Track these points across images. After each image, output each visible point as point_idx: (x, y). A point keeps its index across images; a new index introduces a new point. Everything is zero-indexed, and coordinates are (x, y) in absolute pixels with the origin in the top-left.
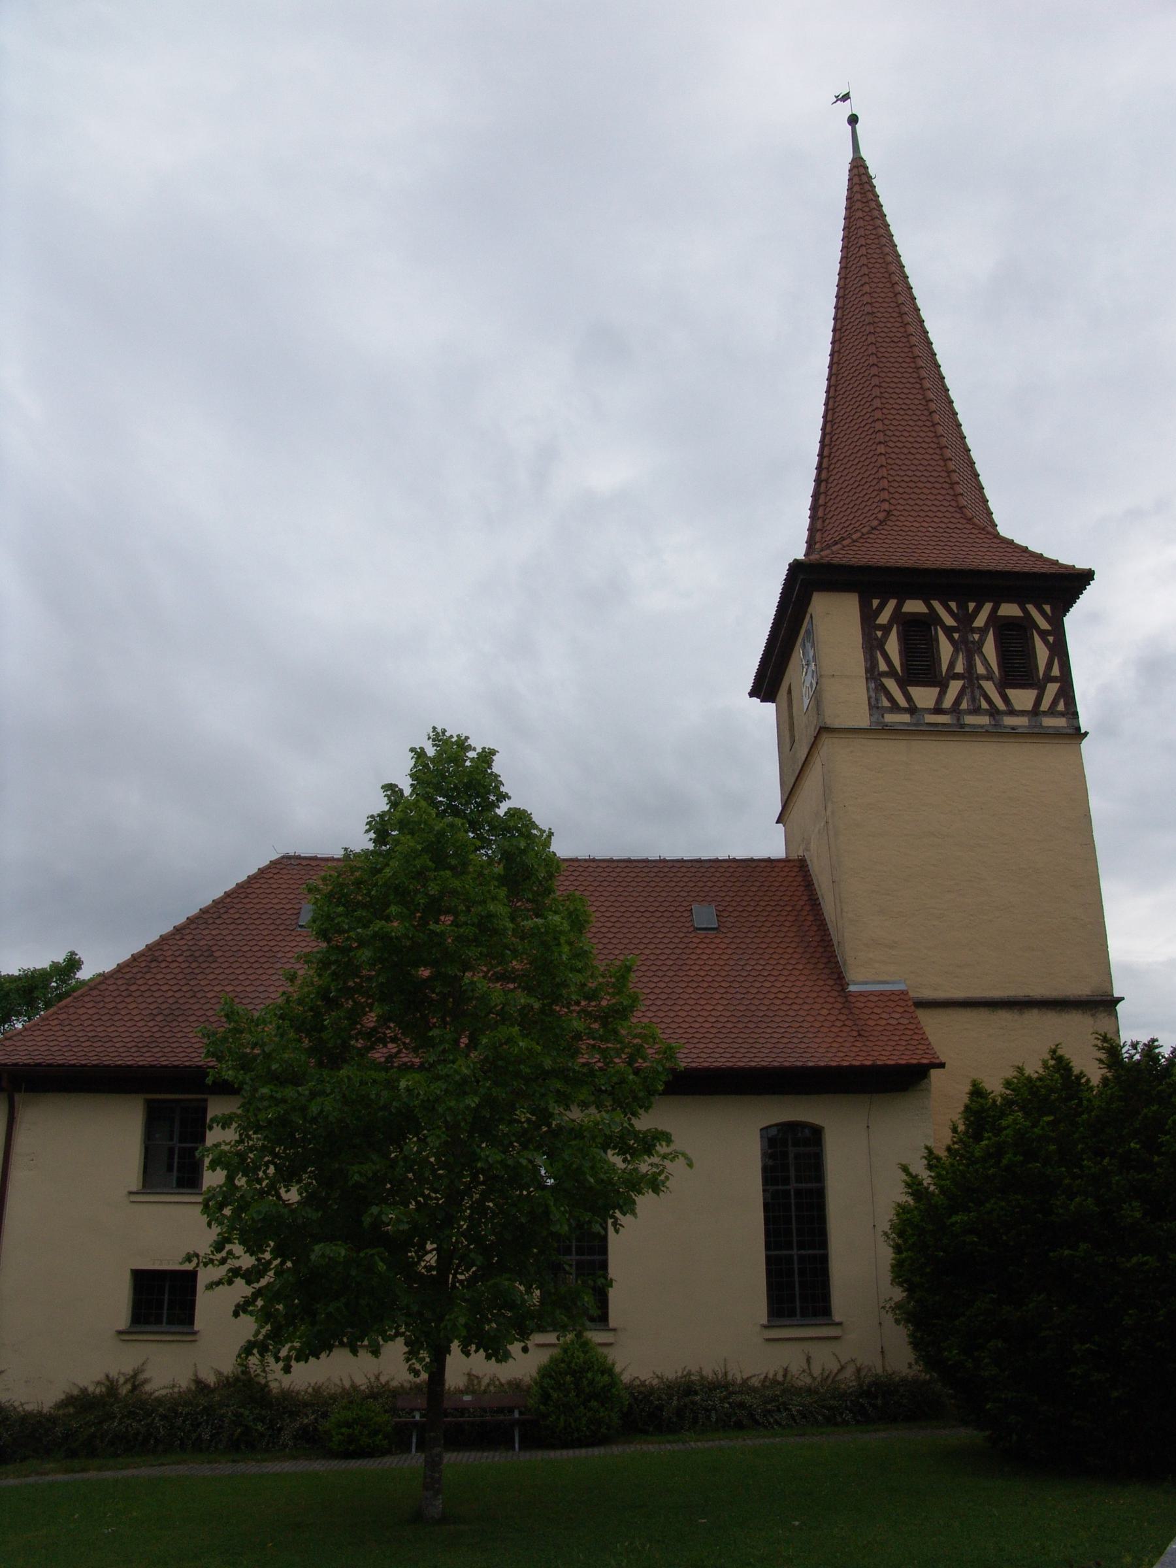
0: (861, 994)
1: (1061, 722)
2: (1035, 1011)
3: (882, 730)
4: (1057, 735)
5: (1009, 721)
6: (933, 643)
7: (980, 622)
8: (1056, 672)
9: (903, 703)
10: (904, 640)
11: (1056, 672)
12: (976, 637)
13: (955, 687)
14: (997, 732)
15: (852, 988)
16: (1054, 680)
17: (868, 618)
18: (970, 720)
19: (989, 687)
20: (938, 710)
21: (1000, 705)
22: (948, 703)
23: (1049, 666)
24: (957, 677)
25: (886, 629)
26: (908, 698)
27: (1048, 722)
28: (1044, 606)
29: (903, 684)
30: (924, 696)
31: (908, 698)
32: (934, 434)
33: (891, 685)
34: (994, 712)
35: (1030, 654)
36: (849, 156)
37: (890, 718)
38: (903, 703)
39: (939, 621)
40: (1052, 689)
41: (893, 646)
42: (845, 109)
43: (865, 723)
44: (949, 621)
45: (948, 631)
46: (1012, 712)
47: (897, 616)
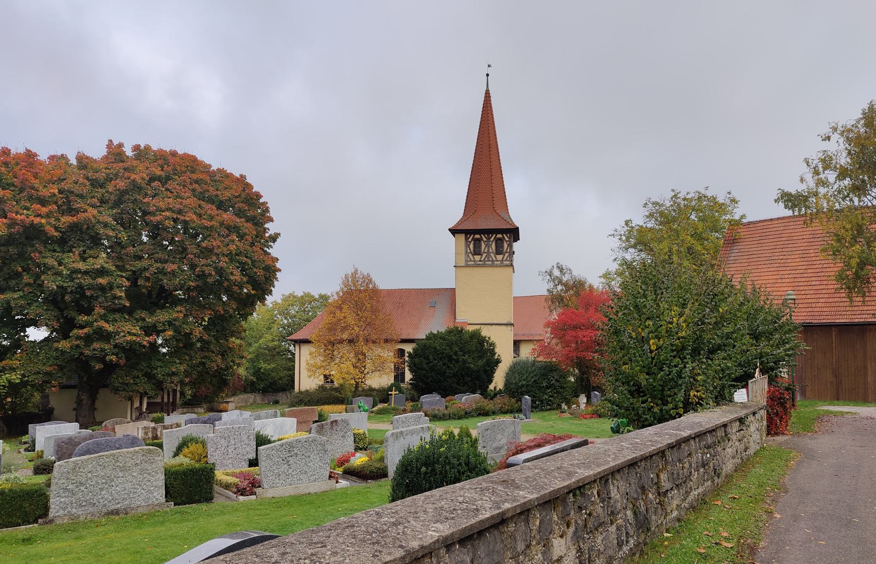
1: (508, 262)
3: (467, 266)
4: (507, 266)
5: (496, 263)
7: (492, 239)
8: (508, 251)
9: (472, 259)
10: (474, 244)
11: (508, 251)
13: (484, 255)
14: (492, 266)
17: (467, 239)
18: (487, 263)
20: (480, 261)
21: (494, 259)
22: (482, 259)
23: (507, 249)
24: (485, 253)
25: (470, 242)
26: (474, 258)
27: (505, 263)
29: (473, 255)
30: (477, 258)
31: (474, 258)
33: (470, 255)
34: (493, 261)
35: (502, 247)
37: (469, 263)
38: (472, 259)
39: (482, 239)
40: (507, 255)
41: (472, 246)
43: (464, 265)
44: (485, 239)
45: (485, 242)
46: (497, 261)
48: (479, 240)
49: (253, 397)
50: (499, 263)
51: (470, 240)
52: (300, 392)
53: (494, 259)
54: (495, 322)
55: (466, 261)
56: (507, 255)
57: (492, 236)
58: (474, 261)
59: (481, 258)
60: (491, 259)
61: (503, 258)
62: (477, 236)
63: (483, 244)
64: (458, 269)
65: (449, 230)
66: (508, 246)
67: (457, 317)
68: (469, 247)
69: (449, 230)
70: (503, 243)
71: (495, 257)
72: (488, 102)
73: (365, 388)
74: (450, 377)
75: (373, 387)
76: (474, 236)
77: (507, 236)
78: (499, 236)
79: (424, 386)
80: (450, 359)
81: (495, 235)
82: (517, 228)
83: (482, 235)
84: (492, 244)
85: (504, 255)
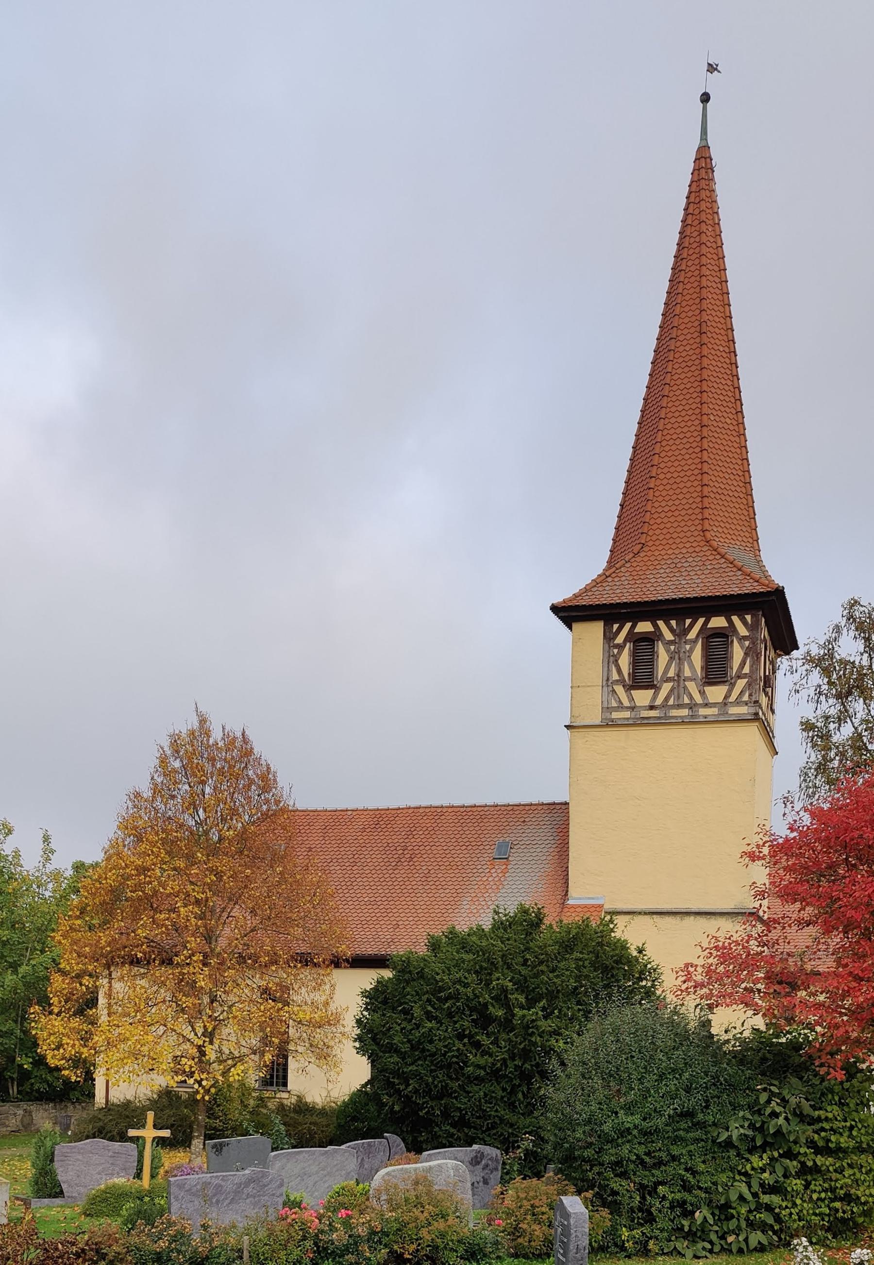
0: (573, 906)
1: (743, 710)
2: (692, 918)
3: (609, 724)
4: (741, 720)
5: (703, 711)
6: (653, 653)
7: (692, 635)
8: (746, 670)
10: (634, 654)
11: (746, 670)
12: (688, 647)
13: (666, 687)
14: (692, 721)
15: (570, 902)
16: (745, 676)
17: (609, 637)
18: (674, 713)
19: (692, 686)
20: (652, 708)
21: (698, 699)
22: (659, 702)
24: (669, 680)
25: (621, 647)
27: (734, 710)
28: (746, 616)
29: (629, 688)
30: (643, 697)
32: (699, 460)
33: (620, 689)
34: (692, 706)
35: (727, 658)
36: (696, 143)
37: (615, 715)
38: (626, 703)
40: (741, 683)
41: (625, 660)
42: (703, 82)
43: (598, 721)
44: (668, 636)
46: (706, 705)
47: (629, 638)
48: (650, 639)
49: (21, 1112)
50: (714, 711)
51: (620, 639)
52: (109, 1107)
53: (698, 699)
54: (694, 907)
55: (607, 709)
56: (741, 683)
57: (692, 626)
58: (632, 708)
59: (655, 697)
60: (686, 700)
61: (726, 697)
62: (645, 627)
63: (661, 649)
64: (578, 733)
65: (555, 609)
66: (747, 654)
67: (572, 892)
68: (616, 662)
69: (555, 609)
70: (727, 645)
71: (702, 693)
72: (703, 194)
73: (285, 1102)
74: (479, 1080)
75: (309, 1099)
76: (633, 627)
77: (745, 623)
78: (718, 622)
79: (397, 1108)
80: (484, 1020)
81: (701, 621)
82: (779, 594)
83: (661, 623)
84: (691, 650)
85: (733, 685)
